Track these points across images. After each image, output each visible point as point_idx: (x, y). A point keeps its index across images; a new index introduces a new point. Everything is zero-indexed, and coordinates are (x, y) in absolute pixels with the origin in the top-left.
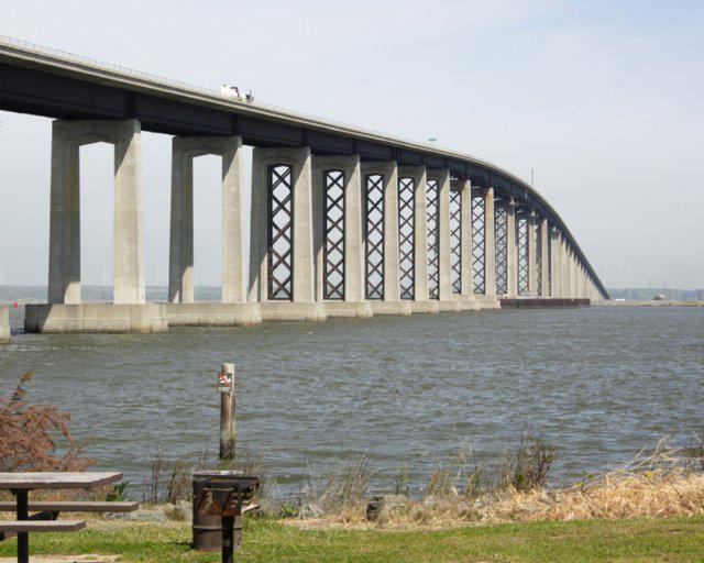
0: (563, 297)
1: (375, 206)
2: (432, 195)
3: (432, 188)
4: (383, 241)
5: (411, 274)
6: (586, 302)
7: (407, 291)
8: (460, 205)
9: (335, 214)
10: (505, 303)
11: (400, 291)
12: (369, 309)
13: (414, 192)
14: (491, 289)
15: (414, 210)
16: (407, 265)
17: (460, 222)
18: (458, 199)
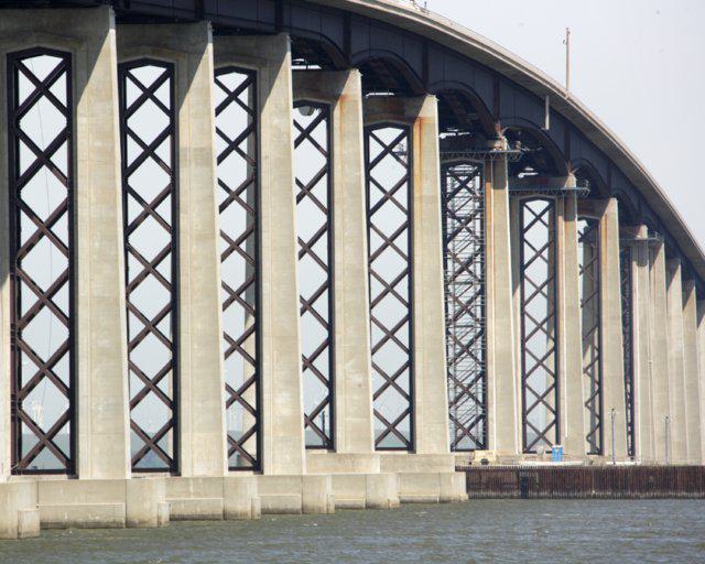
0: (677, 459)
1: (44, 158)
2: (235, 120)
3: (233, 96)
4: (70, 276)
5: (166, 385)
7: (152, 443)
8: (329, 155)
10: (483, 481)
11: (130, 445)
13: (172, 113)
14: (434, 435)
15: (174, 171)
16: (153, 356)
17: (329, 212)
18: (320, 133)
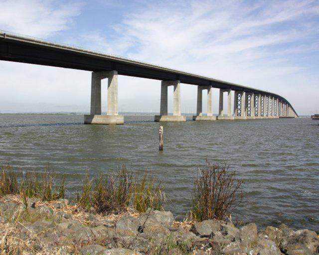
6: (294, 117)
9: (249, 102)
12: (255, 118)
